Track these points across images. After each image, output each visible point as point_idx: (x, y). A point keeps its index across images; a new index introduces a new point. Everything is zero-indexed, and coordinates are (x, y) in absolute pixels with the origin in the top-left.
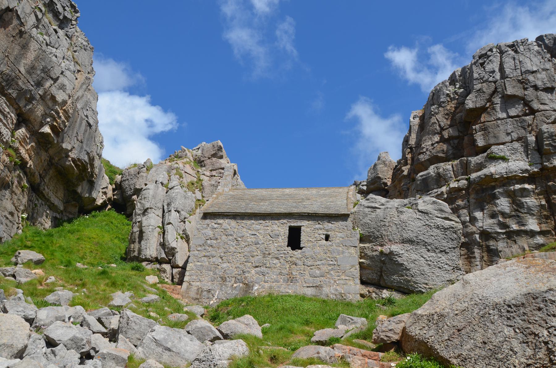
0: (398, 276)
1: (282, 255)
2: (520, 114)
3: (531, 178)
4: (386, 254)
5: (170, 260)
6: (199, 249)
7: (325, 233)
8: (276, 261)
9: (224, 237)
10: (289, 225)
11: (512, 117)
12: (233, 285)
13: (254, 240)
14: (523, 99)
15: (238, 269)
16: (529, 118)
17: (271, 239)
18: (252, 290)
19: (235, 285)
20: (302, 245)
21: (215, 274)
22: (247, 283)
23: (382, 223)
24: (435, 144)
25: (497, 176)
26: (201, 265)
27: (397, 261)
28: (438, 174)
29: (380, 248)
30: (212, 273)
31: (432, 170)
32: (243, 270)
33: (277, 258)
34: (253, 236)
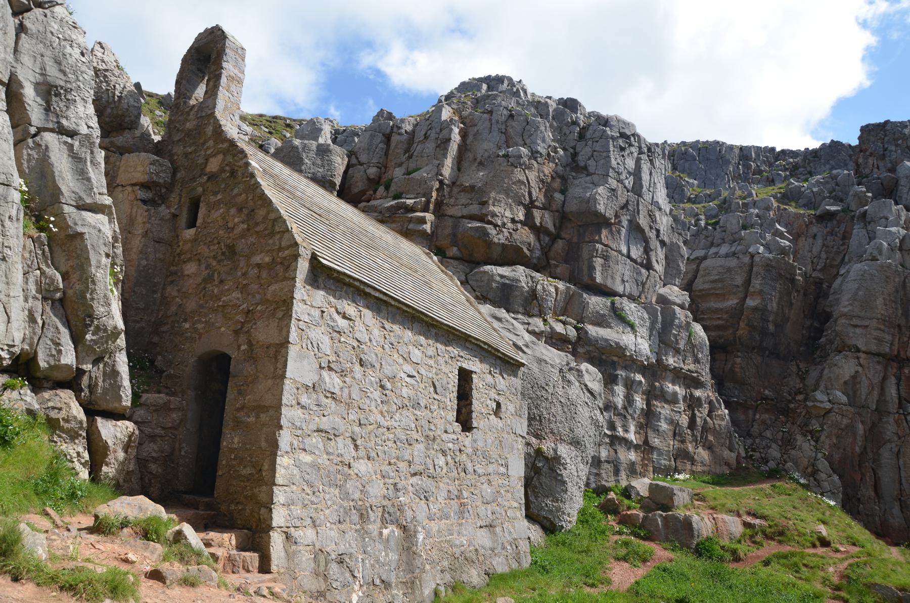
0: (553, 501)
1: (450, 445)
2: (639, 260)
3: (644, 369)
4: (546, 458)
6: (304, 399)
7: (497, 397)
8: (441, 461)
9: (357, 367)
10: (459, 364)
11: (632, 260)
12: (381, 533)
13: (412, 393)
14: (646, 241)
15: (387, 480)
16: (643, 271)
17: (436, 396)
18: (417, 545)
19: (385, 532)
20: (475, 424)
22: (404, 523)
23: (544, 393)
24: (517, 222)
25: (628, 354)
27: (561, 475)
28: (533, 293)
29: (534, 440)
31: (520, 273)
32: (395, 485)
33: (444, 453)
34: (408, 380)
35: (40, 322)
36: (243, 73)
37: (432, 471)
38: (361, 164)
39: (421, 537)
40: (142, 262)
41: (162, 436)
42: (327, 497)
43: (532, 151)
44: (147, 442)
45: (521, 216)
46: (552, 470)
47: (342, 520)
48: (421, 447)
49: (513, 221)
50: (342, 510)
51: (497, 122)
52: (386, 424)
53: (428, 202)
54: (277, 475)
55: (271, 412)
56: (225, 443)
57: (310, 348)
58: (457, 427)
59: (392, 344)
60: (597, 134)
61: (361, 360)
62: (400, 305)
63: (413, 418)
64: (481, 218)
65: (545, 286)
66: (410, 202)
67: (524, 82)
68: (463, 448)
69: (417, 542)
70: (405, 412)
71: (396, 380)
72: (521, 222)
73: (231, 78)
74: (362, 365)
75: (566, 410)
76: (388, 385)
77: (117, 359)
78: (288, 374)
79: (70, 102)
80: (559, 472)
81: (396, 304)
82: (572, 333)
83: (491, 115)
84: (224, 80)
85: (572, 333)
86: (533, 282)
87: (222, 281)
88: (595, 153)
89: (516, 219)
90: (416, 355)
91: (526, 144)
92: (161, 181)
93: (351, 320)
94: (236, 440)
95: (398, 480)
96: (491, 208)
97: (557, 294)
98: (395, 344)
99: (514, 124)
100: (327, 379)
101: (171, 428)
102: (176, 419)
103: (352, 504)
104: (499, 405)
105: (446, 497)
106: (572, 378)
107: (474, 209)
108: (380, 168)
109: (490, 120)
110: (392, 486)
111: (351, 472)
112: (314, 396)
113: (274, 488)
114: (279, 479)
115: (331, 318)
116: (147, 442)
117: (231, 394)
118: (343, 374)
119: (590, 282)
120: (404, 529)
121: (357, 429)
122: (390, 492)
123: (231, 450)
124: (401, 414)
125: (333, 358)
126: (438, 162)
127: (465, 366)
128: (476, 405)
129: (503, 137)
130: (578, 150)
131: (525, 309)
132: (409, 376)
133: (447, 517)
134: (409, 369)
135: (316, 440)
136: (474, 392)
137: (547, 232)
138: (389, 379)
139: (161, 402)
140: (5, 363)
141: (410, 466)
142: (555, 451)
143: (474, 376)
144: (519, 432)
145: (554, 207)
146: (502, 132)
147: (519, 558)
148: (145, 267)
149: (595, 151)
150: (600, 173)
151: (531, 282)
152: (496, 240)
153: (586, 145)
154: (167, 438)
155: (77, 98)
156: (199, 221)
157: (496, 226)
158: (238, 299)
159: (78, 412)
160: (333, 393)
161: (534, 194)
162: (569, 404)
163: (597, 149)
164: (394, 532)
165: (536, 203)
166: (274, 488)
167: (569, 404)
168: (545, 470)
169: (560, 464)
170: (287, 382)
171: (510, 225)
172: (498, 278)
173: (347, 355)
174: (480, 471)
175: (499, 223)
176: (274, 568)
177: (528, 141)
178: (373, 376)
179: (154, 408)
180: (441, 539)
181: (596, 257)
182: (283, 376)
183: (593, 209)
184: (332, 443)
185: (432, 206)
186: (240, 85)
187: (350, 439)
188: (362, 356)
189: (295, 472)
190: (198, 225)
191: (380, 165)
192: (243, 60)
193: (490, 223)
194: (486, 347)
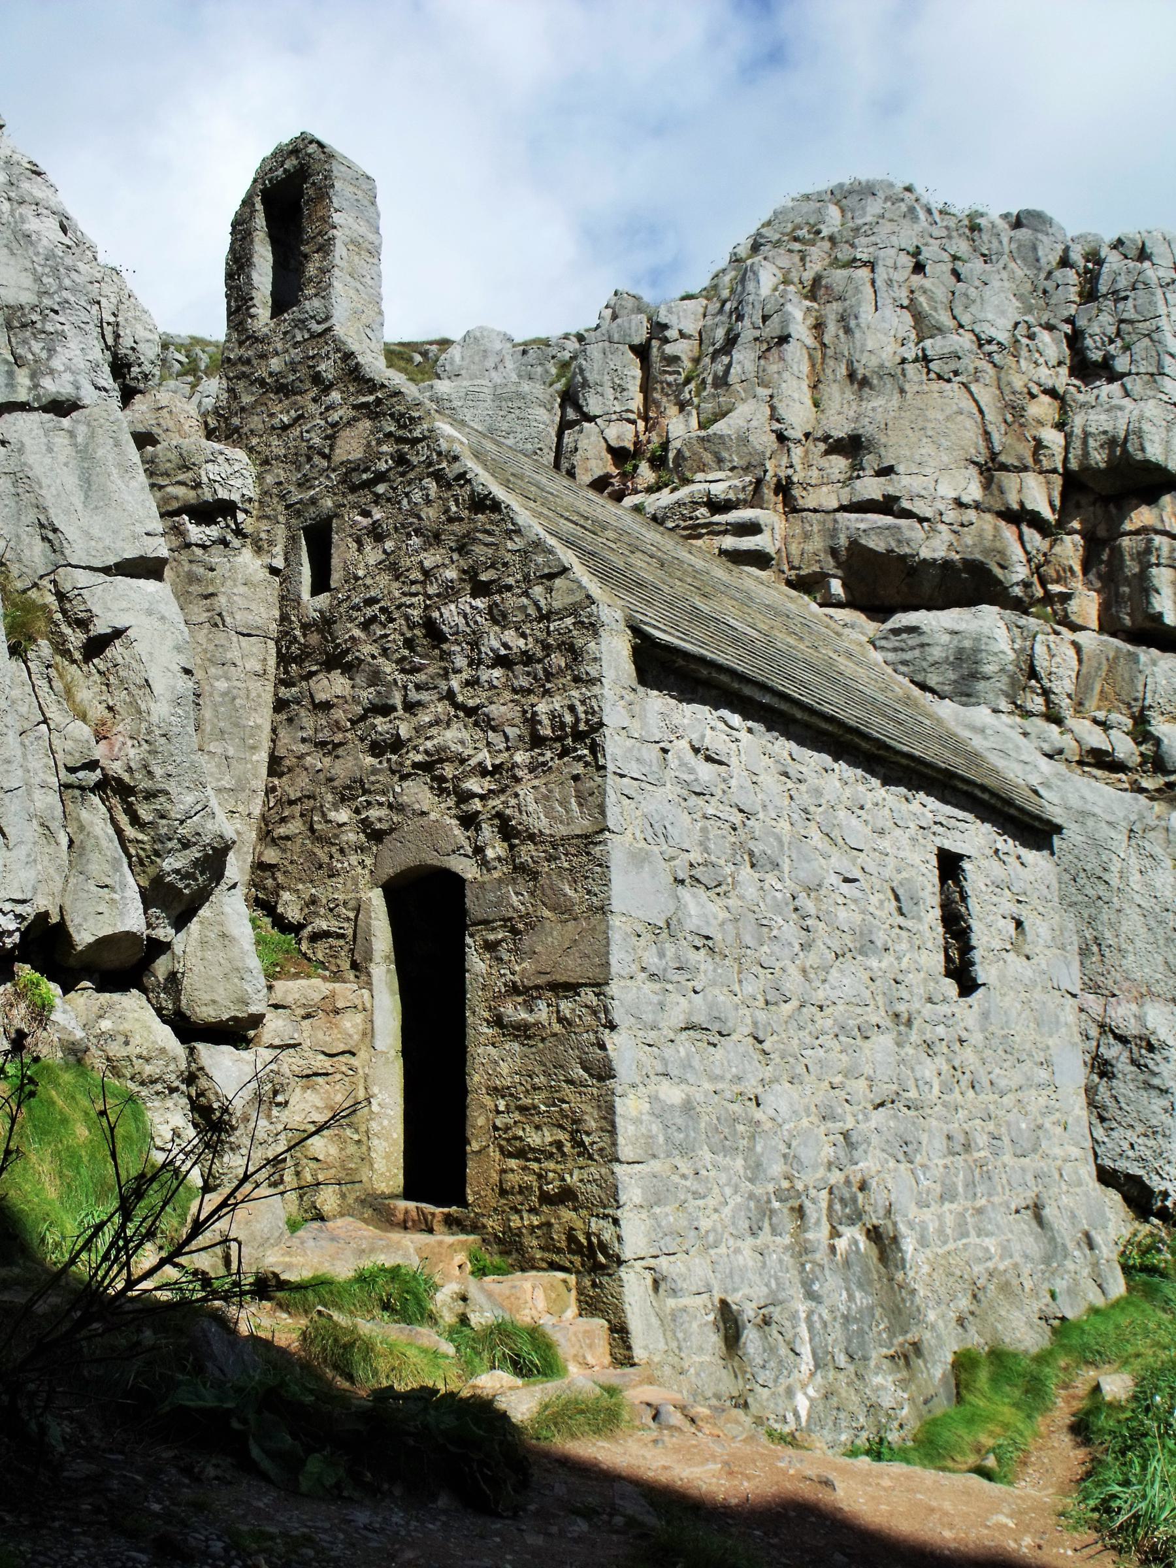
1: (941, 1030)
4: (1122, 1040)
5: (159, 947)
6: (651, 959)
9: (746, 872)
12: (833, 1249)
15: (830, 1125)
17: (900, 920)
21: (756, 1170)
26: (688, 1107)
30: (740, 1162)
32: (846, 1135)
34: (845, 888)
35: (64, 841)
36: (377, 231)
37: (913, 1094)
38: (591, 419)
39: (909, 1245)
40: (217, 684)
41: (327, 1074)
42: (723, 1177)
43: (979, 339)
44: (298, 1090)
45: (974, 491)
46: (1139, 1066)
47: (755, 1227)
48: (885, 1041)
49: (959, 504)
50: (752, 1204)
51: (889, 283)
52: (820, 996)
53: (759, 482)
54: (621, 1140)
55: (588, 996)
56: (476, 1078)
57: (650, 840)
58: (951, 987)
59: (806, 811)
60: (1123, 282)
61: (751, 854)
62: (814, 720)
63: (865, 976)
64: (888, 505)
65: (1052, 646)
66: (718, 490)
67: (920, 190)
68: (964, 1035)
69: (903, 1260)
70: (847, 964)
71: (823, 892)
72: (977, 506)
73: (355, 243)
74: (753, 866)
75: (1153, 924)
76: (810, 906)
77: (227, 909)
78: (616, 905)
79: (53, 340)
80: (1156, 1069)
81: (806, 717)
82: (1124, 747)
83: (873, 271)
84: (340, 250)
85: (1124, 747)
86: (1025, 639)
87: (411, 707)
88: (1123, 326)
89: (966, 499)
90: (855, 829)
91: (961, 326)
92: (235, 497)
93: (721, 763)
94: (504, 1068)
95: (850, 1124)
96: (905, 481)
97: (1080, 661)
98: (812, 809)
99: (927, 283)
100: (693, 908)
101: (343, 1053)
102: (351, 1031)
103: (771, 1188)
104: (1019, 924)
105: (945, 1151)
106: (1158, 850)
107: (871, 488)
108: (633, 422)
109: (873, 282)
110: (841, 1138)
111: (758, 1115)
112: (670, 950)
113: (618, 1168)
114: (625, 1150)
115: (683, 764)
116: (298, 1090)
117: (477, 963)
118: (716, 887)
119: (1148, 625)
120: (874, 1234)
121: (762, 1016)
122: (841, 1154)
123: (496, 1091)
124: (841, 971)
125: (696, 856)
126: (769, 392)
127: (948, 845)
128: (981, 937)
129: (907, 317)
130: (1081, 323)
131: (1014, 703)
132: (847, 880)
133: (953, 1198)
134: (841, 862)
135: (685, 1045)
136: (972, 902)
137: (1035, 520)
138: (809, 890)
139: (317, 997)
140: (9, 942)
141: (871, 1086)
142: (1140, 1018)
143: (966, 865)
144: (1066, 985)
145: (1046, 464)
146: (902, 307)
147: (1099, 1275)
148: (224, 694)
149: (1122, 321)
150: (1142, 370)
151: (1019, 641)
152: (925, 553)
153: (1100, 310)
154: (338, 1076)
155: (66, 328)
156: (336, 578)
157: (922, 520)
158: (462, 742)
159: (165, 1036)
160: (708, 938)
161: (996, 437)
162: (1157, 909)
163: (1125, 316)
164: (856, 1243)
165: (1002, 458)
166: (618, 1168)
167: (1157, 909)
168: (1123, 1066)
169: (1151, 1048)
170: (615, 921)
171: (951, 515)
172: (946, 638)
173: (721, 844)
174: (1002, 1083)
175: (929, 513)
176: (639, 1354)
177: (965, 319)
178: (779, 886)
179: (302, 1012)
180: (946, 1248)
181: (1158, 565)
182: (603, 910)
183: (1139, 456)
184: (718, 1054)
185: (768, 493)
186: (375, 261)
187: (750, 1039)
188: (752, 845)
189: (654, 1128)
190: (333, 585)
191: (632, 416)
192: (373, 203)
193: (907, 514)
194: (986, 796)
